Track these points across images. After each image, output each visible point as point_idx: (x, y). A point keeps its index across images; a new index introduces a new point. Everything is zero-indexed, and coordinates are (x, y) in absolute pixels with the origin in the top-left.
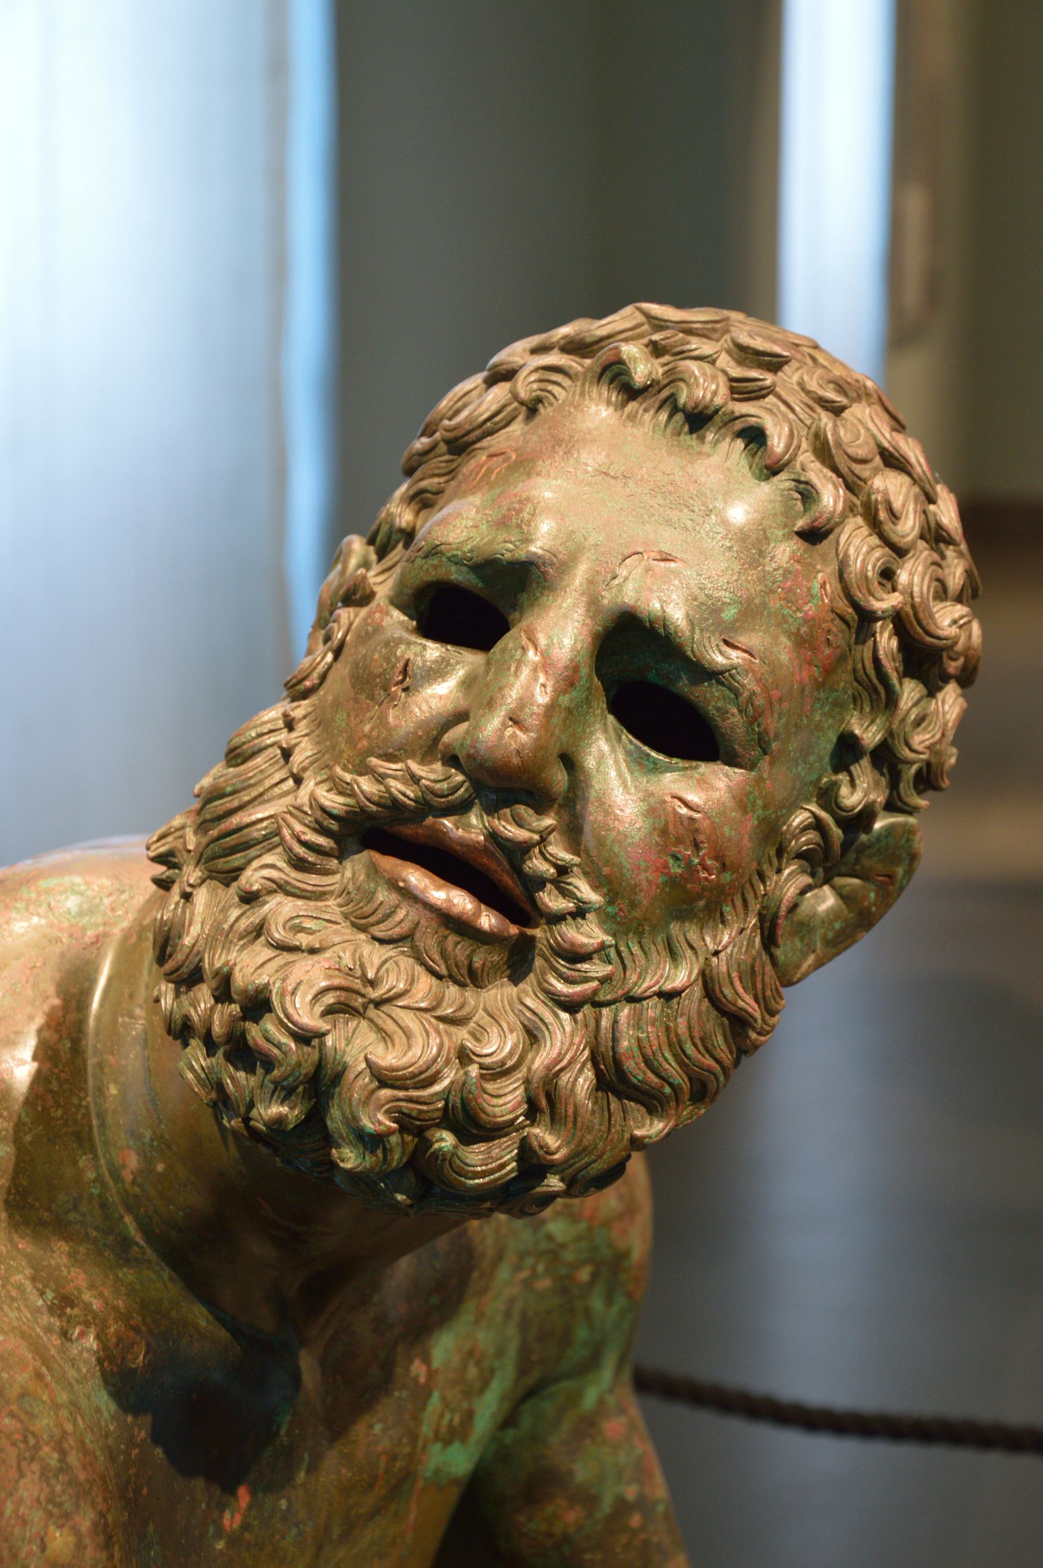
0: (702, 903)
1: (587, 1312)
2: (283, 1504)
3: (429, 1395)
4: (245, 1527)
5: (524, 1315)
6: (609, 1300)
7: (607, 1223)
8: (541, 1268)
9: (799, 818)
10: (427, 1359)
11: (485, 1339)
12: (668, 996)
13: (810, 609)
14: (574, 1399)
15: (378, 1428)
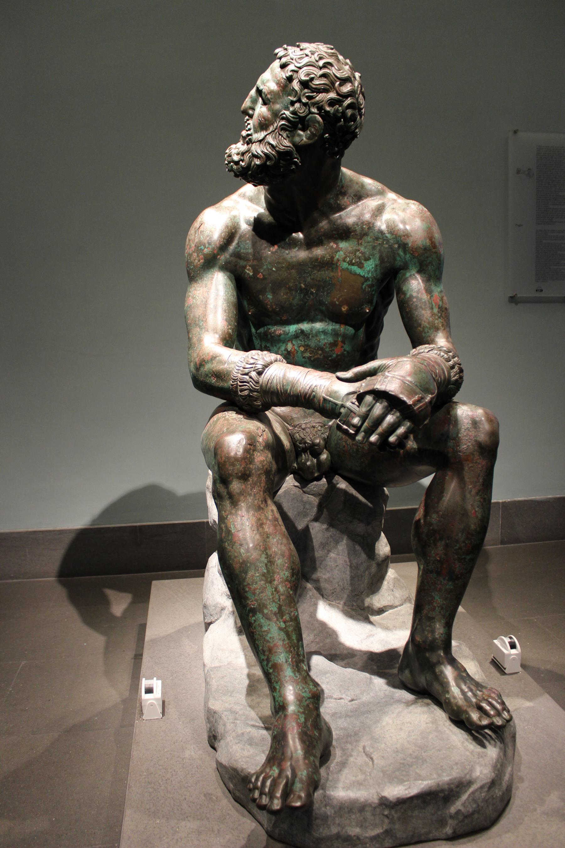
0: (264, 127)
1: (398, 254)
2: (287, 252)
3: (339, 251)
4: (276, 252)
5: (380, 250)
6: (405, 253)
7: (400, 236)
8: (385, 243)
9: (282, 112)
10: (337, 244)
11: (362, 249)
12: (260, 141)
13: (279, 79)
14: (404, 275)
15: (319, 251)
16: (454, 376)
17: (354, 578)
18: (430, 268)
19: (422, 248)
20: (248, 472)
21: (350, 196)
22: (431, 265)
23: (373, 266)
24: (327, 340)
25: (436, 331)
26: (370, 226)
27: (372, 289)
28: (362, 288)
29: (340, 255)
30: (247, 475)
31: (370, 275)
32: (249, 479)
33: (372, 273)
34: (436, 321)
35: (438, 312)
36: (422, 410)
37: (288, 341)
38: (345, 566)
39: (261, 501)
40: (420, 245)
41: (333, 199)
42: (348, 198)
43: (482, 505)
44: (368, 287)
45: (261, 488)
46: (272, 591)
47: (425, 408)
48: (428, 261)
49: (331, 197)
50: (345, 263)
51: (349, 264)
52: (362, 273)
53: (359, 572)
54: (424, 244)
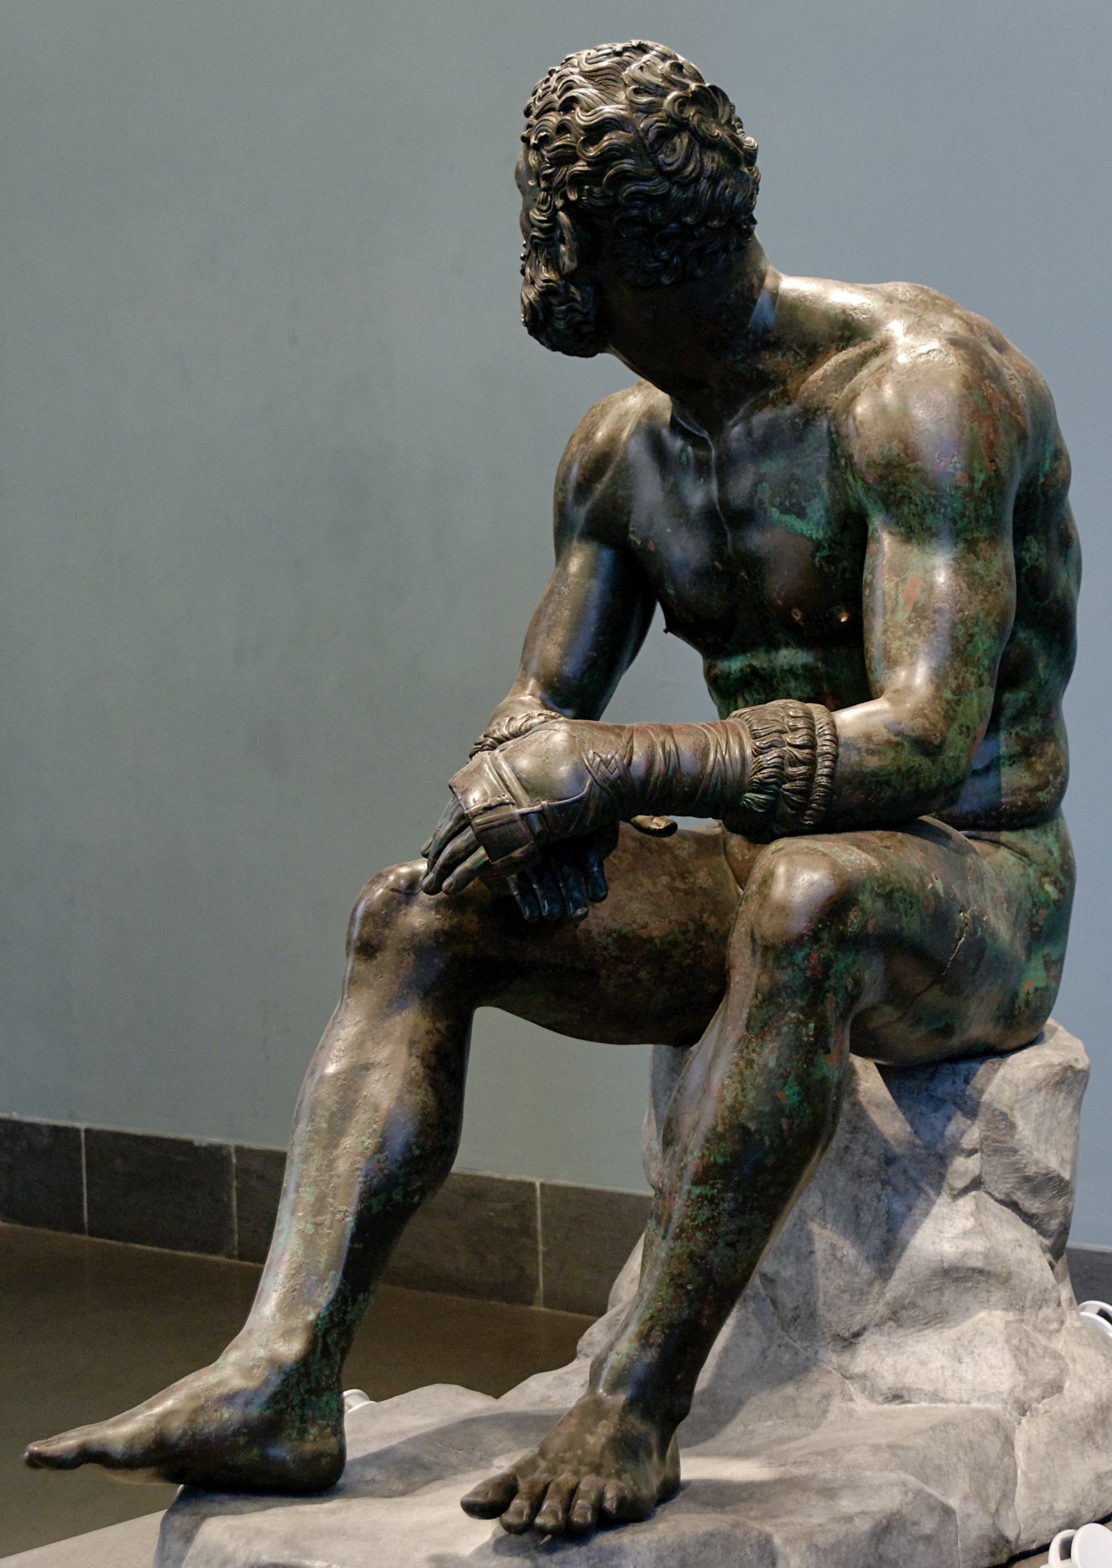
6: (856, 482)
16: (755, 774)
17: (844, 1292)
18: (906, 510)
19: (879, 464)
20: (375, 942)
21: (790, 349)
22: (906, 501)
23: (822, 512)
24: (802, 691)
25: (888, 668)
26: (808, 419)
27: (840, 567)
28: (814, 565)
29: (765, 492)
30: (372, 947)
31: (821, 533)
32: (377, 955)
33: (823, 528)
34: (897, 643)
35: (909, 620)
36: (494, 827)
37: (737, 692)
38: (831, 1258)
39: (390, 1001)
40: (875, 457)
41: (743, 361)
42: (784, 355)
43: (741, 1073)
44: (828, 562)
45: (398, 976)
46: (321, 1165)
47: (501, 825)
48: (899, 494)
49: (739, 357)
50: (774, 510)
51: (781, 512)
52: (808, 533)
53: (857, 1280)
54: (885, 453)
